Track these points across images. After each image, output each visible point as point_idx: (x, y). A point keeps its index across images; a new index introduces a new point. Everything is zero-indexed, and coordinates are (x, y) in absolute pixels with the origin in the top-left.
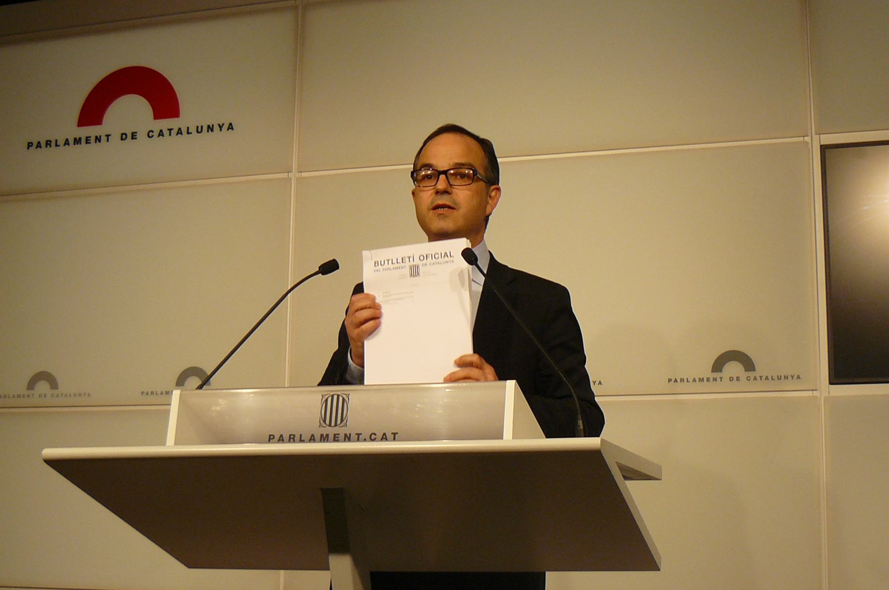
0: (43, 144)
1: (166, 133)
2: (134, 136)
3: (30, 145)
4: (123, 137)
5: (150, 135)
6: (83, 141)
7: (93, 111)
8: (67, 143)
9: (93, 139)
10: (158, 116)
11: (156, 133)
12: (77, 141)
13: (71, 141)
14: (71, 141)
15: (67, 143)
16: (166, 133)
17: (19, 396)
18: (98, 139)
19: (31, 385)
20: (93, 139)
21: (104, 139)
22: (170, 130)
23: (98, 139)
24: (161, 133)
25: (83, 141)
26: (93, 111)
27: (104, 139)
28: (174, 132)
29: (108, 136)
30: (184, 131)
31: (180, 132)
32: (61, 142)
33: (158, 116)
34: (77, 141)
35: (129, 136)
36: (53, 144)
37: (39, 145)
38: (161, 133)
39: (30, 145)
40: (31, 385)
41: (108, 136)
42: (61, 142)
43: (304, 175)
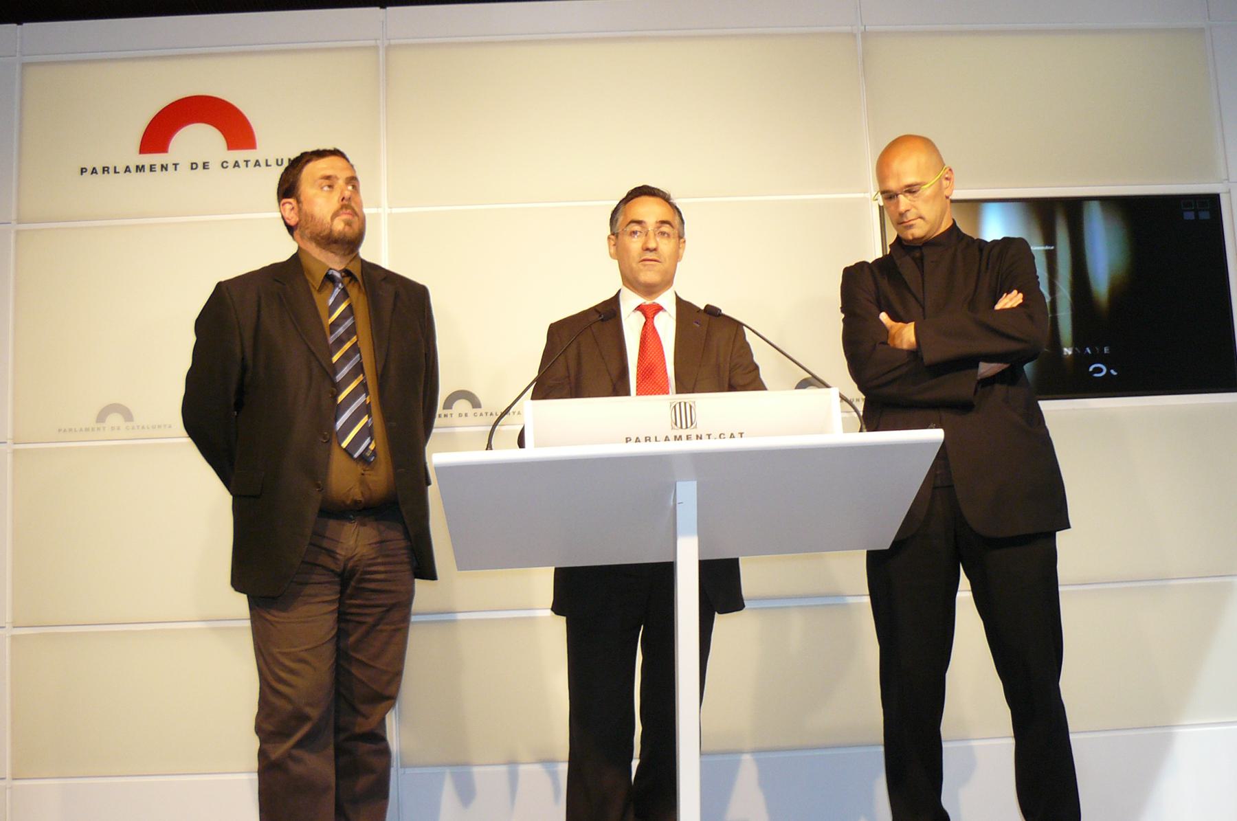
0: (99, 170)
1: (242, 164)
2: (205, 166)
3: (83, 171)
4: (194, 166)
5: (223, 165)
6: (147, 168)
7: (157, 136)
8: (127, 169)
9: (158, 168)
10: (232, 145)
11: (231, 164)
12: (140, 169)
13: (133, 169)
14: (133, 169)
15: (127, 169)
16: (242, 164)
17: (87, 430)
18: (164, 167)
19: (102, 417)
20: (158, 168)
21: (171, 168)
22: (247, 162)
23: (164, 167)
24: (236, 165)
25: (147, 168)
26: (157, 136)
27: (171, 168)
28: (251, 164)
29: (175, 165)
30: (263, 163)
31: (257, 164)
32: (121, 169)
33: (232, 145)
34: (140, 169)
35: (201, 166)
36: (111, 170)
37: (94, 171)
38: (236, 165)
39: (83, 171)
40: (102, 417)
41: (175, 165)
42: (121, 169)
43: (395, 210)
